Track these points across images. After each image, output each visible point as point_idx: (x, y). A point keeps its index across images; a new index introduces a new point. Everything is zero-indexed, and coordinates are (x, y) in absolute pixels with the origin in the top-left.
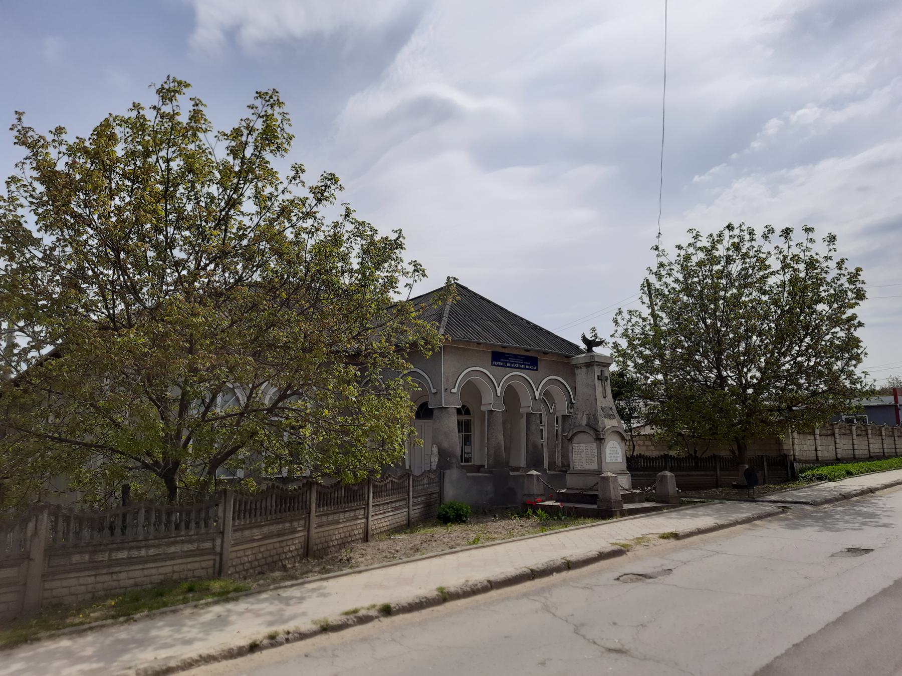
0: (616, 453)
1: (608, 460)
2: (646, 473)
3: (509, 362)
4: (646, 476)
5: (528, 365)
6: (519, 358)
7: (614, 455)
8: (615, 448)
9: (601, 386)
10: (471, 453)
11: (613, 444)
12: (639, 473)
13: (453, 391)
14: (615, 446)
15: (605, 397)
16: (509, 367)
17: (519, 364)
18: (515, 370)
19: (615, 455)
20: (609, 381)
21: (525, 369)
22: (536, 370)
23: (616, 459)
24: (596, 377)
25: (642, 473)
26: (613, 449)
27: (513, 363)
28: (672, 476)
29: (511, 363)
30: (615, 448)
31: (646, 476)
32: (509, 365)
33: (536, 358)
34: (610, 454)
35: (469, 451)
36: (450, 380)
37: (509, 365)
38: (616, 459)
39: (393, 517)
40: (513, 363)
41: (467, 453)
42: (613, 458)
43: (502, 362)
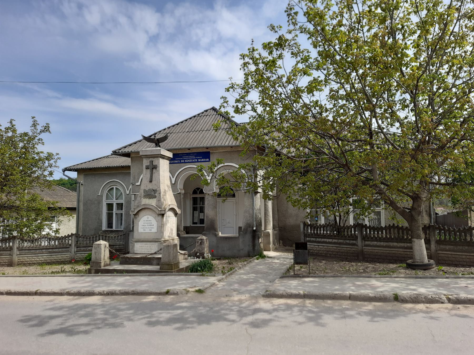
0: (151, 225)
1: (141, 230)
2: (336, 241)
3: (182, 160)
4: (335, 243)
5: (200, 159)
6: (192, 155)
8: (150, 221)
11: (148, 218)
12: (328, 240)
13: (137, 184)
14: (149, 219)
15: (151, 181)
16: (183, 163)
17: (191, 159)
18: (189, 164)
19: (150, 227)
21: (198, 162)
22: (209, 161)
23: (151, 230)
24: (144, 167)
25: (330, 240)
26: (146, 222)
27: (186, 159)
29: (185, 160)
30: (150, 221)
31: (335, 243)
32: (183, 161)
33: (209, 152)
36: (136, 178)
37: (183, 161)
38: (151, 230)
39: (50, 256)
40: (186, 159)
42: (146, 229)
43: (177, 160)
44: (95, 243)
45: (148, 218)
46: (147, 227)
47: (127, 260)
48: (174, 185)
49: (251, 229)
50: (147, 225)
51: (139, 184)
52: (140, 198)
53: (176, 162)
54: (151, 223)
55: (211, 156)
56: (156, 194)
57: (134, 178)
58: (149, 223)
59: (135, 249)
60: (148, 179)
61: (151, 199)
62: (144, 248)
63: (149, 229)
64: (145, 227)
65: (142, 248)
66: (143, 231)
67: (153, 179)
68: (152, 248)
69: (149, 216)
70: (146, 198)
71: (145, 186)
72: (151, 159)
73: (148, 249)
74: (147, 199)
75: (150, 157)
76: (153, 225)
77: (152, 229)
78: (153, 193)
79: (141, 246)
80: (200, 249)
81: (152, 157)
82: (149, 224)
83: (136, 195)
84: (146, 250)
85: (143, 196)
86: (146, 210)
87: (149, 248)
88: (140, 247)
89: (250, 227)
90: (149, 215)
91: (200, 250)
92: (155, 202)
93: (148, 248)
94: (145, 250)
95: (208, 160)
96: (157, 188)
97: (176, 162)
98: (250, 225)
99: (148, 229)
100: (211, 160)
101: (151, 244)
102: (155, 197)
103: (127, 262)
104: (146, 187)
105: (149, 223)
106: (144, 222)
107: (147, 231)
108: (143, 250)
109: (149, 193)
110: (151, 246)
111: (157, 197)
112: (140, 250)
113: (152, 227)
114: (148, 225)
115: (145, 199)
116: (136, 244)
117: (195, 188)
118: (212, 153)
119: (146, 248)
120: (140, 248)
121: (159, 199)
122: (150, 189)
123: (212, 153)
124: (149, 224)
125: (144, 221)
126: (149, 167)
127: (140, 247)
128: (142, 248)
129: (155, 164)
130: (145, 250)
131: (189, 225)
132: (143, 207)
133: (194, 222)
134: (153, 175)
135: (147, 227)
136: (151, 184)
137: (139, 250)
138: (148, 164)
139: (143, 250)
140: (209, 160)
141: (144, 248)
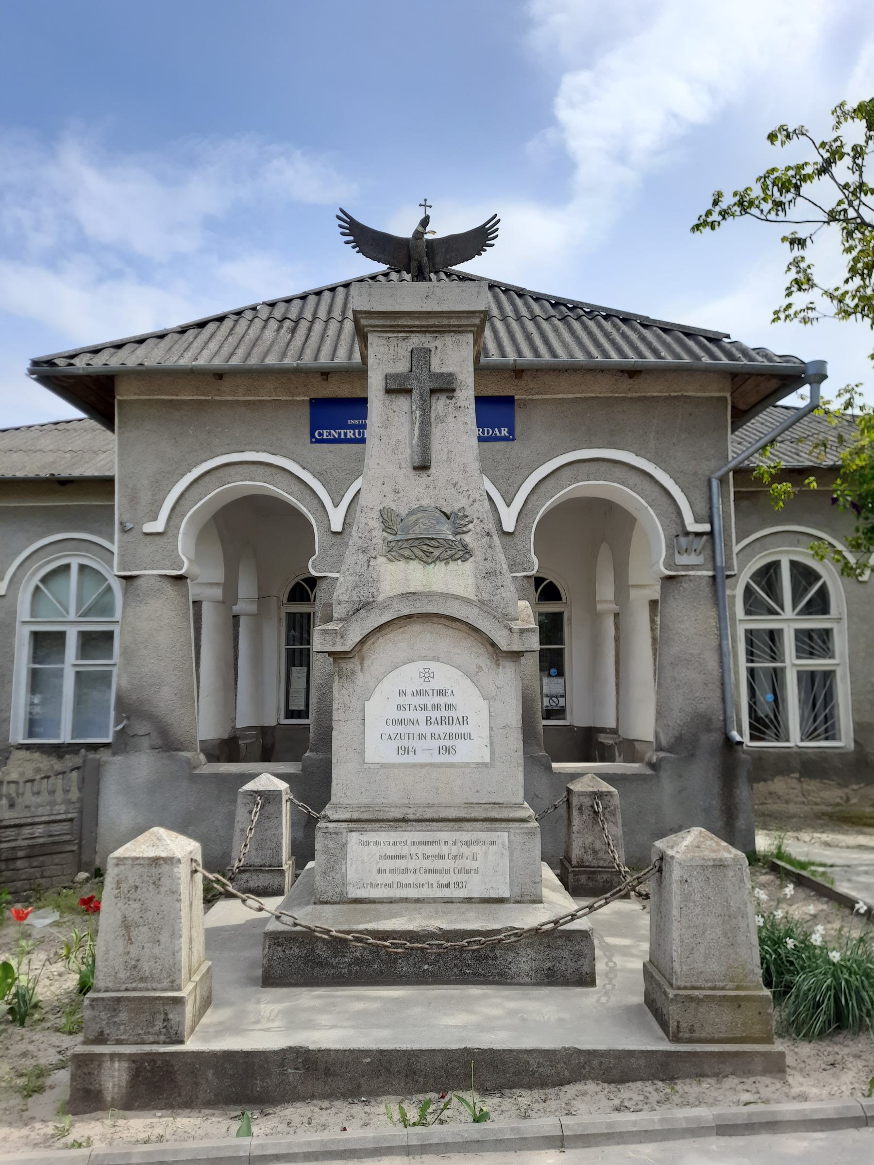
0: (449, 721)
7: (423, 728)
8: (441, 693)
9: (405, 420)
10: (563, 696)
11: (427, 676)
13: (149, 528)
14: (436, 684)
15: (423, 467)
20: (466, 395)
22: (511, 437)
23: (448, 750)
28: (720, 865)
30: (441, 693)
34: (401, 722)
35: (561, 692)
36: (145, 497)
38: (448, 750)
41: (551, 697)
44: (120, 852)
45: (427, 676)
46: (427, 730)
47: (321, 951)
48: (337, 539)
49: (716, 737)
50: (421, 716)
51: (158, 526)
52: (362, 558)
53: (350, 434)
54: (449, 707)
55: (520, 417)
56: (467, 538)
57: (133, 500)
58: (437, 707)
59: (352, 875)
60: (407, 454)
61: (440, 566)
62: (412, 864)
63: (437, 743)
64: (412, 729)
65: (401, 864)
66: (392, 757)
67: (437, 454)
68: (474, 865)
69: (433, 666)
70: (408, 558)
71: (387, 489)
72: (416, 341)
73: (441, 871)
74: (415, 565)
75: (411, 330)
76: (464, 720)
77: (460, 744)
78: (446, 531)
79: (391, 851)
80: (598, 845)
81: (424, 330)
82: (435, 715)
83: (139, 582)
84: (433, 878)
85: (381, 547)
86: (416, 628)
87: (447, 864)
88: (386, 857)
89: (709, 730)
90: (436, 659)
91: (595, 852)
92: (471, 580)
93: (439, 864)
94: (423, 878)
95: (504, 432)
96: (463, 502)
97: (350, 434)
98: (710, 720)
99: (429, 743)
100: (516, 437)
101: (465, 836)
102: (466, 553)
103: (322, 964)
104: (391, 496)
105: (437, 707)
106: (402, 700)
107: (421, 758)
108: (410, 878)
109: (418, 531)
110: (465, 850)
111: (479, 555)
112: (388, 878)
113: (455, 729)
114: (427, 721)
115: (401, 564)
116: (354, 837)
117: (298, 579)
118: (525, 404)
119: (428, 864)
120: (388, 864)
121: (489, 565)
122: (421, 509)
123: (525, 404)
124: (435, 715)
125: (402, 693)
126: (414, 384)
127: (386, 857)
128: (401, 864)
129: (445, 370)
130: (423, 878)
131: (273, 723)
132: (406, 611)
133: (292, 707)
134: (437, 432)
135: (427, 730)
136: (423, 479)
137: (380, 879)
138: (402, 367)
139: (410, 878)
140: (511, 432)
141: (412, 864)
